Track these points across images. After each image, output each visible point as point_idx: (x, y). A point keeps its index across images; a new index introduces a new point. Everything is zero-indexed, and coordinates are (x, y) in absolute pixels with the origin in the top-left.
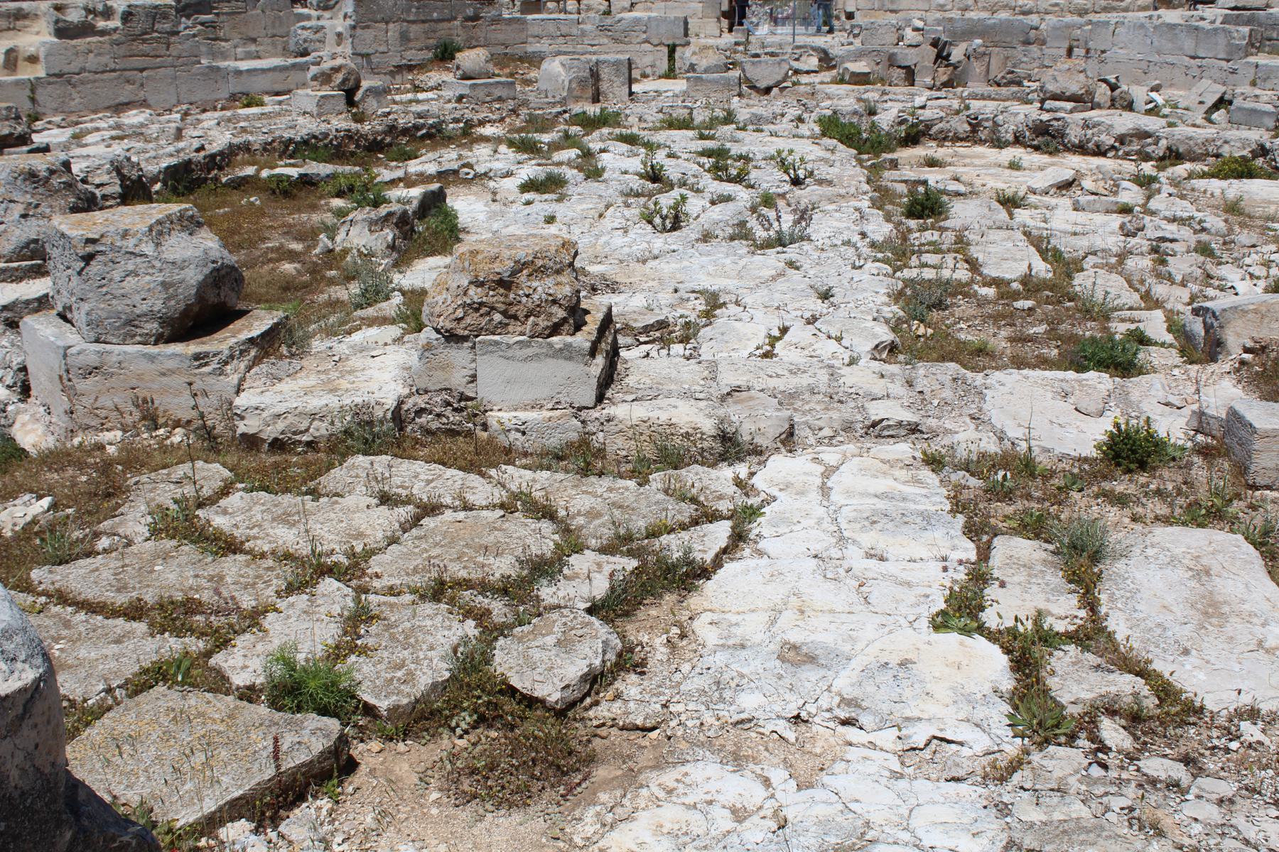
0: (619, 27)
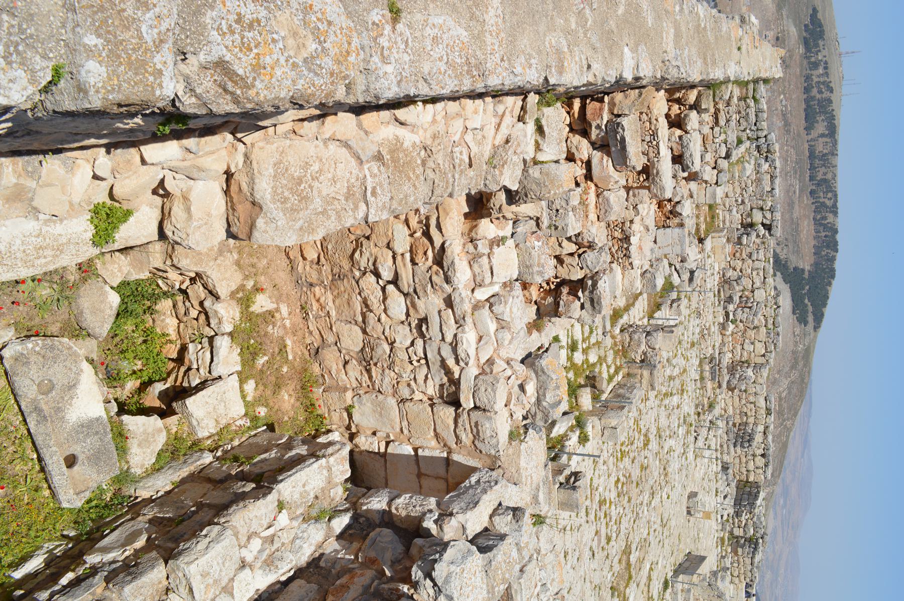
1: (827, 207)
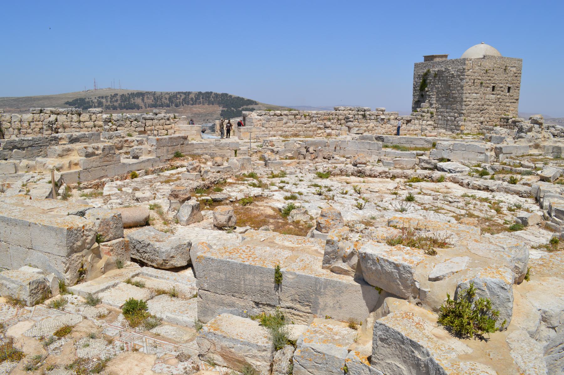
0: (221, 145)
1: (185, 98)
